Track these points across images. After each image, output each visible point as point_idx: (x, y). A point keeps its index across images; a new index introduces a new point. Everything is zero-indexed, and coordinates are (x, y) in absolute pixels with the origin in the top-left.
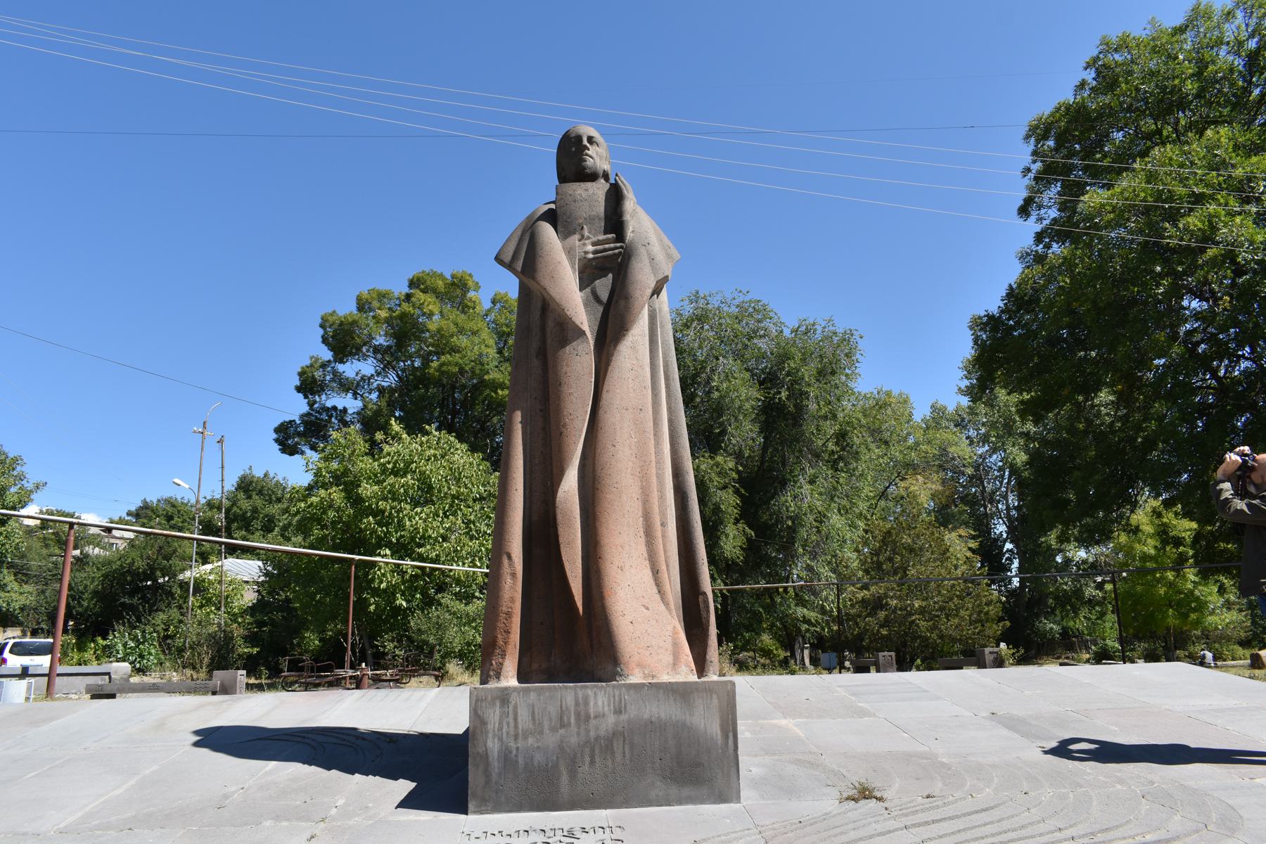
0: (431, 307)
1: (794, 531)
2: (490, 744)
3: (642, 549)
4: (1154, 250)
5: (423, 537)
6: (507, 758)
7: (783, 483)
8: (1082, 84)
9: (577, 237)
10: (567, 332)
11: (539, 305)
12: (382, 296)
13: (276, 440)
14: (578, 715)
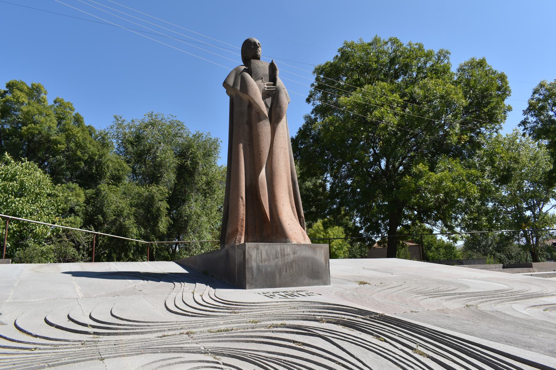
0: (23, 99)
1: (187, 222)
2: (253, 264)
4: (363, 122)
5: (20, 213)
6: (258, 268)
7: (184, 201)
8: (337, 56)
10: (260, 116)
11: (247, 104)
14: (281, 254)
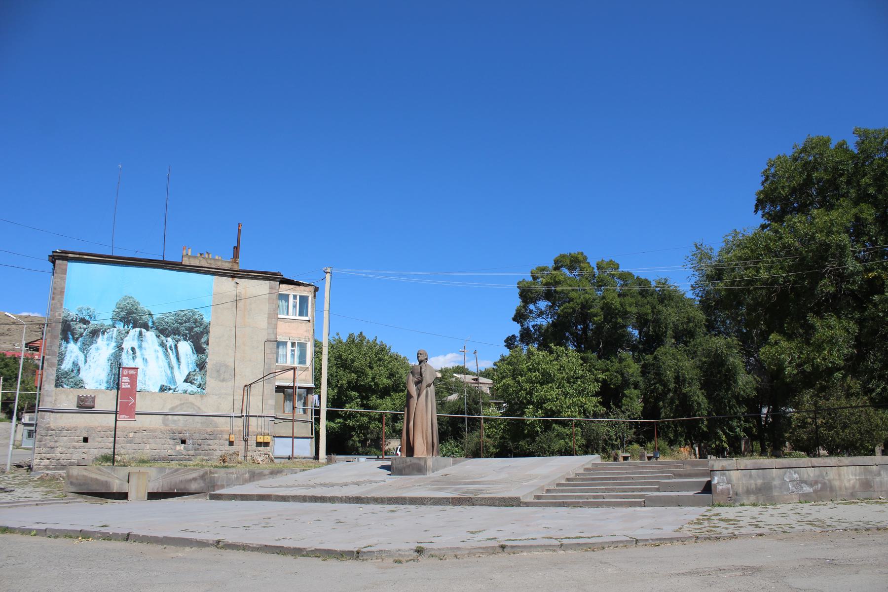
12: (543, 270)
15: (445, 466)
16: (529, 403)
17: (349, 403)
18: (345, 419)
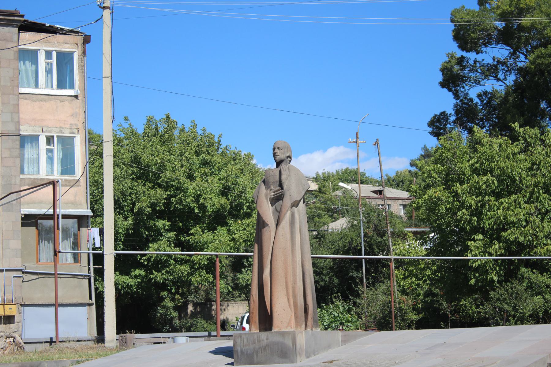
3: (285, 292)
6: (242, 352)
9: (269, 190)
13: (432, 133)
15: (329, 347)
16: (476, 230)
17: (155, 240)
18: (149, 269)
